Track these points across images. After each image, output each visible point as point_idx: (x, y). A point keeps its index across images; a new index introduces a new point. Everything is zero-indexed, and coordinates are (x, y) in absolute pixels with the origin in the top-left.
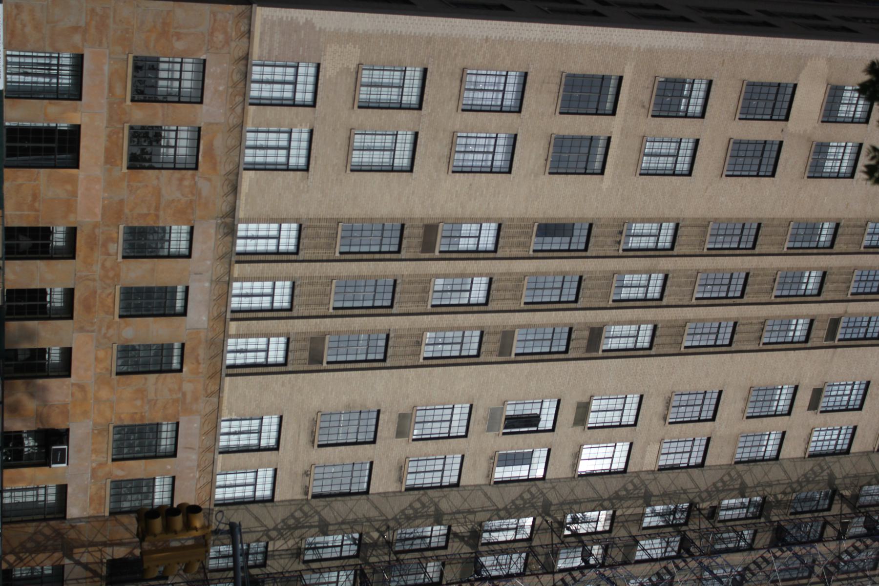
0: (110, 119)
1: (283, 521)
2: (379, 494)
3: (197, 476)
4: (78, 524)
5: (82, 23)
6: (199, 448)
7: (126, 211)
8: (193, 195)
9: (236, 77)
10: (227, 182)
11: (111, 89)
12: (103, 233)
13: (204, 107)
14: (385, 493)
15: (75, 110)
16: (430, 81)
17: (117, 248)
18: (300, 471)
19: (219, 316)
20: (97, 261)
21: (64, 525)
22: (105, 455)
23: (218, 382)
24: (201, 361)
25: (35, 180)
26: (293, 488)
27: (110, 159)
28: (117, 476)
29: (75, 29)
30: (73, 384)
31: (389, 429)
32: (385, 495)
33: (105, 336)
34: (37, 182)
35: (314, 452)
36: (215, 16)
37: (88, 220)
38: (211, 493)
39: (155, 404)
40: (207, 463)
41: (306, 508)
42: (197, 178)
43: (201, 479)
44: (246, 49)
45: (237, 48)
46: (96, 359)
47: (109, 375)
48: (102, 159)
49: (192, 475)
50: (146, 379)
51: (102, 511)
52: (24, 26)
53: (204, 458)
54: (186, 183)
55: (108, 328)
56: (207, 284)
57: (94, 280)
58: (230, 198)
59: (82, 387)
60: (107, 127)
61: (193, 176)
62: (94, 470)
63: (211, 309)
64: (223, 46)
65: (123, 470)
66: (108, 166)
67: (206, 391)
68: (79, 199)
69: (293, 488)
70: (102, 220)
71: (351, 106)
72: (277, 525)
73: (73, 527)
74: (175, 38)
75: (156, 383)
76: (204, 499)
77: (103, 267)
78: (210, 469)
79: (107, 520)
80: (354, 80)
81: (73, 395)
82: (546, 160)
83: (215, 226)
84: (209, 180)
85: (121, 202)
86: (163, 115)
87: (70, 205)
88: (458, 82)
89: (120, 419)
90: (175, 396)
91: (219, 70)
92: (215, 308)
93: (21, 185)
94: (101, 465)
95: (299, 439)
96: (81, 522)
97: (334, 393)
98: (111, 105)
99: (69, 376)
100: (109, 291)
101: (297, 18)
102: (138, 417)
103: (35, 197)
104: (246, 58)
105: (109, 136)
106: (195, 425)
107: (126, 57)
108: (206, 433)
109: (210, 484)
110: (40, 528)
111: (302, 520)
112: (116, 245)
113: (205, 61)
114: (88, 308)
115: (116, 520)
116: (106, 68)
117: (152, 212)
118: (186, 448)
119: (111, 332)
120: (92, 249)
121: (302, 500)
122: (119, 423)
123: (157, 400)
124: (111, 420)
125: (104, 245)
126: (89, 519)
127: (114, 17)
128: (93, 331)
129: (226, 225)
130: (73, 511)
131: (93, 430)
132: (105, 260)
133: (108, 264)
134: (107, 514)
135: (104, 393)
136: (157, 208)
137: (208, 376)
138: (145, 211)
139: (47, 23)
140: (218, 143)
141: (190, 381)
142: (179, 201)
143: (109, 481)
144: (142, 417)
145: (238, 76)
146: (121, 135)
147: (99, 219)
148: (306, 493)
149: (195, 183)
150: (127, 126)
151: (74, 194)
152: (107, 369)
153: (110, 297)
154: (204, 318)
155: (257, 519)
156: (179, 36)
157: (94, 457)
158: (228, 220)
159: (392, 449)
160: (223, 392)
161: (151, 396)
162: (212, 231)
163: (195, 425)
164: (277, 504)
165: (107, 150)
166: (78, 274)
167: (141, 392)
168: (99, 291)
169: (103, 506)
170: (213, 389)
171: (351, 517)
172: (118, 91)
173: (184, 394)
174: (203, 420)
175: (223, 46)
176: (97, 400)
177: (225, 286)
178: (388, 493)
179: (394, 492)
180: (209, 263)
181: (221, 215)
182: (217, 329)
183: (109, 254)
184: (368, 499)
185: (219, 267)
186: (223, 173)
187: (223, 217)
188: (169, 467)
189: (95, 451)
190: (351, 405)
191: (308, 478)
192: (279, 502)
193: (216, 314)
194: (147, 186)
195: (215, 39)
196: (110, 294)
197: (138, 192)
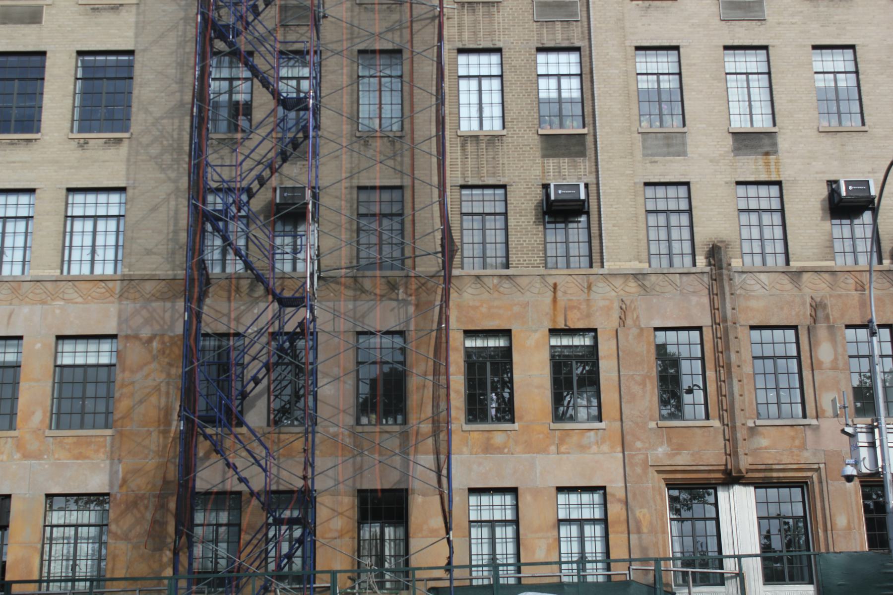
1: (162, 170)
2: (137, 36)
3: (62, 303)
4: (121, 475)
6: (11, 304)
14: (137, 26)
18: (79, 153)
21: (119, 496)
26: (104, 161)
28: (42, 422)
31: (23, 35)
32: (140, 28)
35: (45, 137)
38: (103, 280)
40: (37, 291)
41: (145, 140)
43: (66, 296)
49: (58, 311)
51: (102, 439)
53: (31, 296)
62: (26, 456)
65: (33, 413)
69: (104, 161)
72: (169, 179)
73: (124, 481)
76: (103, 290)
78: (48, 285)
79: (121, 434)
94: (19, 445)
96: (117, 472)
109: (76, 283)
110: (119, 532)
111: (165, 143)
115: (122, 418)
118: (8, 324)
121: (130, 147)
126: (114, 457)
130: (96, 483)
134: (109, 432)
143: (48, 433)
148: (119, 140)
155: (154, 209)
159: (59, 26)
164: (131, 182)
169: (93, 439)
171: (172, 71)
178: (137, 23)
179: (138, 14)
184: (144, 50)
191: (91, 142)
192: (128, 179)
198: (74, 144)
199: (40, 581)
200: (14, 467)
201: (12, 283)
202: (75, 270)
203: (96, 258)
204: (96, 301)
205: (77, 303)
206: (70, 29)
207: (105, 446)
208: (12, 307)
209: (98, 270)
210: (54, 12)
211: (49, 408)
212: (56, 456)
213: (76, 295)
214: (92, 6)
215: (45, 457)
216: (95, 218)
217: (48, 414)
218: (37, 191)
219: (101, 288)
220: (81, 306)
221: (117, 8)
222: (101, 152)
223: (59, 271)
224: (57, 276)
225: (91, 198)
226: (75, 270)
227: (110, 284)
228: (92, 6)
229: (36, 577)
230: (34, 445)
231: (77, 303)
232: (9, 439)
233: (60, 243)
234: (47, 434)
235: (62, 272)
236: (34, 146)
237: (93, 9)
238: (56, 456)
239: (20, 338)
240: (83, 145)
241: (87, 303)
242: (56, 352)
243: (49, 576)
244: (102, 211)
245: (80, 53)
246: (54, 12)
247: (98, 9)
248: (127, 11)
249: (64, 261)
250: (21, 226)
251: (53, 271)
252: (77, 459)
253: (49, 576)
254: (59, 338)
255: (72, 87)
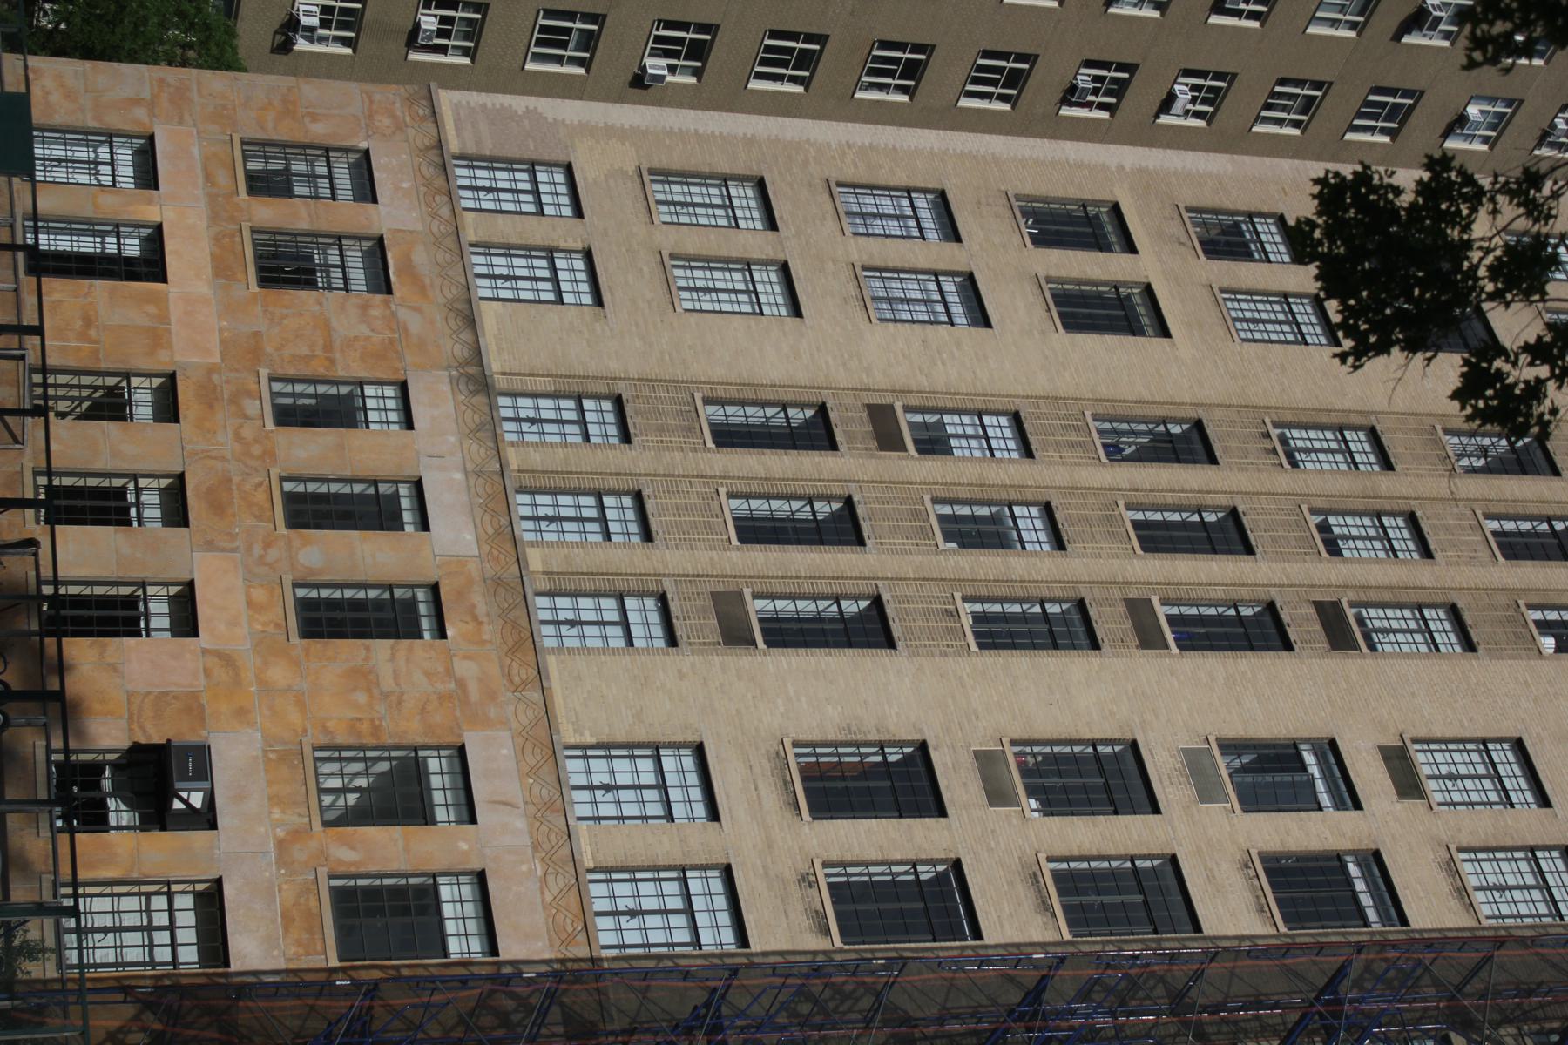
0: (214, 218)
3: (539, 872)
5: (147, 94)
6: (526, 803)
7: (269, 349)
8: (393, 331)
9: (429, 171)
10: (452, 315)
11: (208, 177)
12: (228, 382)
13: (380, 206)
15: (150, 202)
16: (775, 193)
17: (260, 409)
18: (791, 876)
19: (498, 532)
20: (225, 427)
22: (304, 810)
23: (531, 658)
24: (485, 619)
25: (86, 296)
27: (222, 270)
28: (340, 862)
29: (136, 102)
30: (205, 651)
31: (965, 784)
33: (261, 561)
34: (90, 300)
35: (806, 829)
36: (370, 97)
37: (195, 360)
39: (399, 703)
40: (553, 837)
42: (393, 307)
43: (551, 879)
44: (436, 135)
45: (422, 135)
46: (250, 603)
47: (285, 637)
48: (209, 271)
49: (524, 868)
50: (368, 649)
51: (319, 948)
52: (48, 93)
54: (375, 313)
55: (267, 545)
56: (459, 476)
57: (223, 459)
58: (466, 336)
59: (227, 659)
60: (209, 227)
61: (387, 304)
62: (281, 845)
63: (478, 521)
64: (394, 133)
65: (353, 848)
66: (222, 281)
67: (511, 681)
68: (174, 328)
70: (223, 360)
71: (648, 220)
74: (307, 120)
75: (393, 658)
76: (570, 929)
77: (238, 437)
78: (566, 851)
80: (639, 187)
81: (207, 673)
82: (1049, 310)
83: (447, 380)
84: (418, 310)
85: (257, 334)
86: (310, 215)
87: (157, 337)
88: (826, 196)
89: (326, 731)
90: (440, 687)
91: (394, 162)
92: (487, 518)
93: (60, 301)
94: (297, 834)
95: (758, 796)
97: (803, 699)
98: (212, 198)
99: (196, 635)
100: (257, 480)
101: (510, 106)
102: (365, 727)
103: (88, 322)
104: (439, 145)
105: (217, 240)
106: (504, 751)
107: (228, 138)
108: (534, 771)
109: (575, 889)
112: (258, 402)
113: (367, 153)
114: (218, 508)
116: (196, 151)
117: (317, 353)
118: (495, 802)
119: (273, 554)
120: (211, 407)
122: (323, 740)
123: (402, 694)
124: (305, 731)
125: (234, 400)
127: (199, 91)
128: (233, 550)
129: (469, 377)
131: (265, 752)
132: (241, 426)
133: (248, 433)
135: (279, 674)
136: (328, 347)
137: (506, 648)
138: (305, 351)
139: (86, 91)
140: (420, 257)
141: (466, 657)
142: (368, 338)
143: (323, 872)
144: (376, 730)
145: (431, 169)
146: (238, 239)
147: (217, 359)
148: (827, 933)
149: (394, 314)
150: (246, 226)
151: (164, 318)
152: (277, 625)
153: (261, 489)
154: (469, 537)
156: (315, 118)
157: (277, 814)
158: (472, 370)
160: (548, 678)
161: (387, 683)
162: (445, 388)
163: (504, 751)
165: (214, 257)
166: (188, 447)
167: (363, 677)
168: (236, 479)
170: (524, 677)
172: (222, 178)
173: (461, 683)
174: (521, 740)
175: (394, 133)
176: (265, 686)
177: (498, 479)
180: (452, 439)
181: (456, 364)
182: (502, 557)
183: (246, 417)
185: (475, 447)
186: (442, 300)
187: (461, 365)
188: (464, 846)
189: (275, 800)
190: (854, 728)
191: (814, 892)
193: (491, 531)
194: (301, 315)
195: (377, 124)
196: (260, 484)
197: (285, 322)
198: (806, 868)
199: (75, 884)
200: (263, 829)
201: (560, 800)
202: (597, 890)
203: (624, 919)
204: (550, 920)
205: (542, 893)
206: (993, 845)
207: (308, 954)
208: (521, 805)
209: (603, 923)
210: (1015, 821)
211: (363, 870)
212: (285, 887)
213: (555, 891)
214: (1039, 873)
215: (283, 871)
216: (689, 911)
217: (353, 870)
218: (716, 824)
219: (572, 925)
220: (539, 900)
221: (1046, 909)
222: (800, 907)
223: (591, 865)
224: (582, 861)
225: (721, 902)
226: (597, 890)
227: (582, 938)
228: (1039, 873)
229: (83, 875)
230: (299, 853)
231: (542, 893)
232: (307, 819)
233: (638, 862)
234: (319, 869)
235: (589, 871)
236: (789, 815)
237: (1035, 875)
238: (285, 887)
239: (473, 820)
240: (807, 880)
241: (544, 908)
242: (457, 874)
243: (85, 896)
244: (702, 919)
245: (957, 865)
246: (1015, 821)
247: (1038, 882)
248: (1044, 923)
249: (608, 871)
250: (656, 809)
251: (590, 857)
252: (283, 916)
253: (85, 896)
254: (481, 878)
255: (898, 856)
